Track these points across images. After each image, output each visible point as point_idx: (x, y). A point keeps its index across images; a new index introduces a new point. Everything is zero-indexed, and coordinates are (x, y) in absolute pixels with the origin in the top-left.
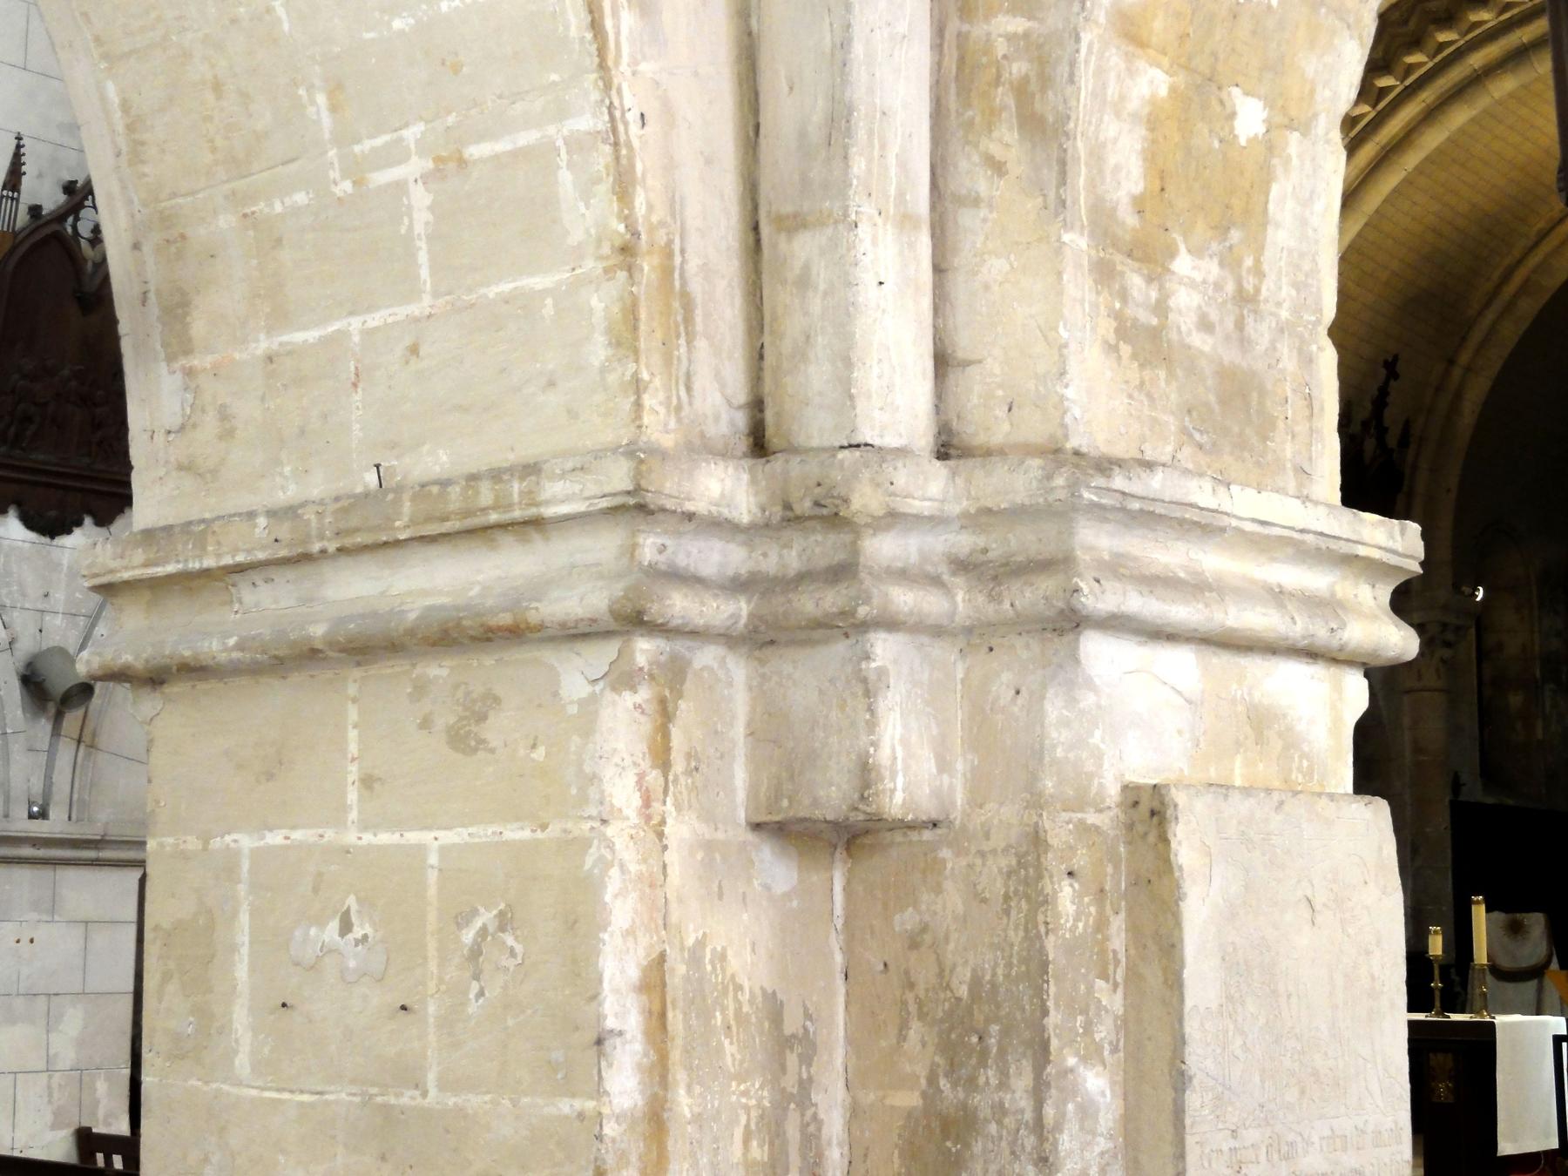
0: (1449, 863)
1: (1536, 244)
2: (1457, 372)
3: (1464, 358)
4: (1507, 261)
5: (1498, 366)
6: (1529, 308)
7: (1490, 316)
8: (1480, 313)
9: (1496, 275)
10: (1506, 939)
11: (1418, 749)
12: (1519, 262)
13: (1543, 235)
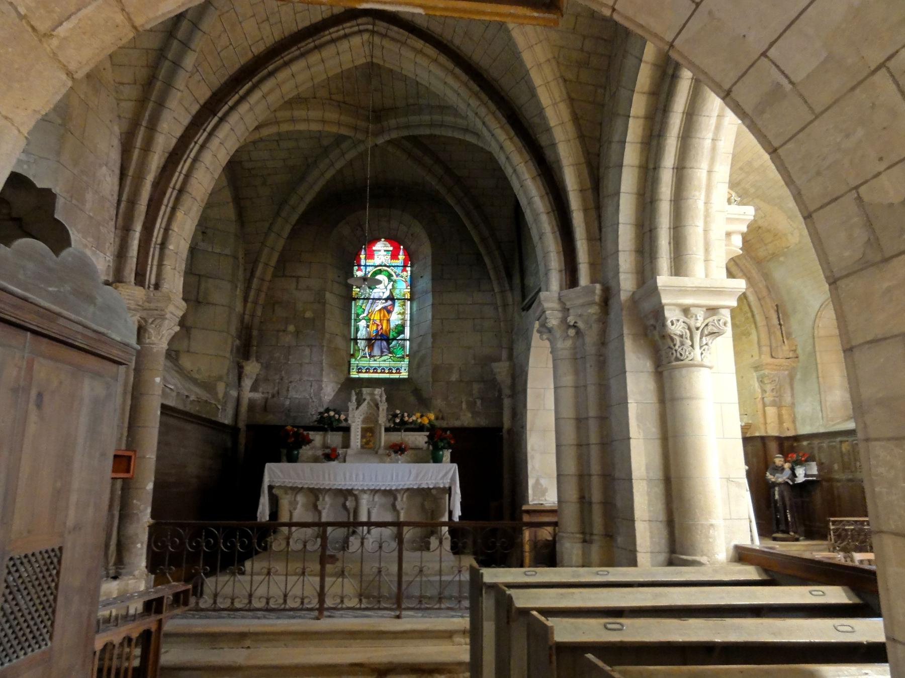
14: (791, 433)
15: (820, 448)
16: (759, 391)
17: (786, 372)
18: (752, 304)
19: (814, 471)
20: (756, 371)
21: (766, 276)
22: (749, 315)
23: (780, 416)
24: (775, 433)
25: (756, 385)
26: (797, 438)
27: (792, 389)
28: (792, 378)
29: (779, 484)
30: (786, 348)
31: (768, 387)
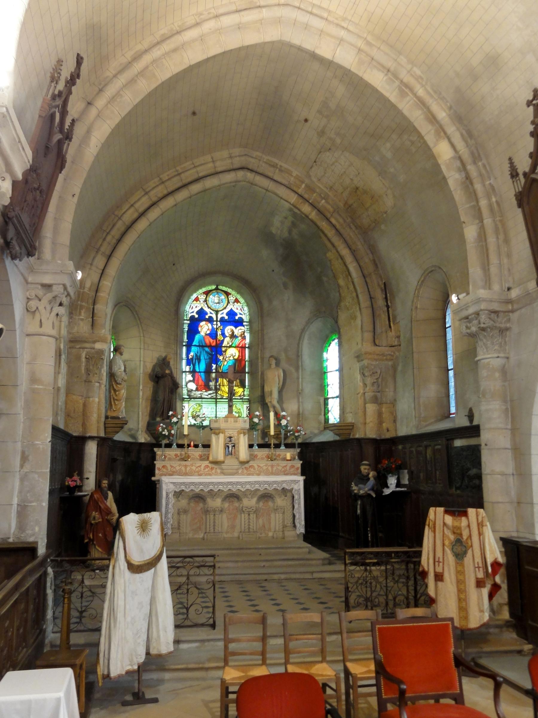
0: (48, 470)
1: (158, 43)
2: (93, 112)
3: (100, 103)
4: (139, 48)
5: (117, 120)
6: (144, 87)
7: (122, 79)
8: (115, 76)
9: (129, 55)
10: (138, 537)
11: (34, 379)
12: (146, 51)
13: (165, 39)
14: (388, 436)
15: (411, 452)
16: (361, 384)
17: (390, 363)
18: (356, 281)
19: (405, 481)
20: (359, 361)
21: (373, 249)
22: (354, 294)
23: (380, 414)
24: (372, 434)
25: (359, 377)
26: (395, 441)
27: (395, 382)
28: (395, 368)
29: (362, 497)
30: (392, 334)
31: (369, 381)
